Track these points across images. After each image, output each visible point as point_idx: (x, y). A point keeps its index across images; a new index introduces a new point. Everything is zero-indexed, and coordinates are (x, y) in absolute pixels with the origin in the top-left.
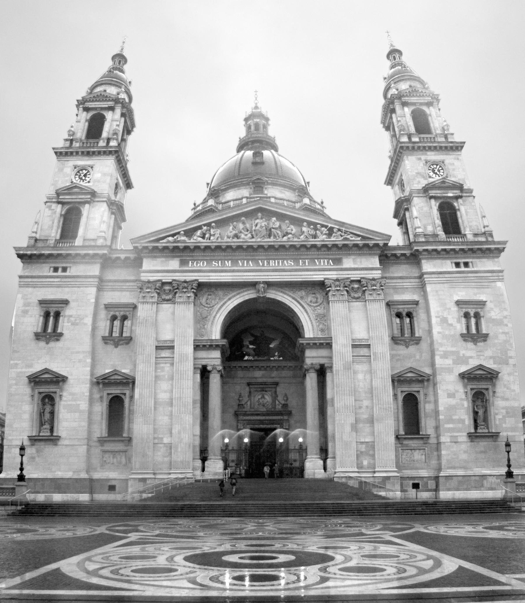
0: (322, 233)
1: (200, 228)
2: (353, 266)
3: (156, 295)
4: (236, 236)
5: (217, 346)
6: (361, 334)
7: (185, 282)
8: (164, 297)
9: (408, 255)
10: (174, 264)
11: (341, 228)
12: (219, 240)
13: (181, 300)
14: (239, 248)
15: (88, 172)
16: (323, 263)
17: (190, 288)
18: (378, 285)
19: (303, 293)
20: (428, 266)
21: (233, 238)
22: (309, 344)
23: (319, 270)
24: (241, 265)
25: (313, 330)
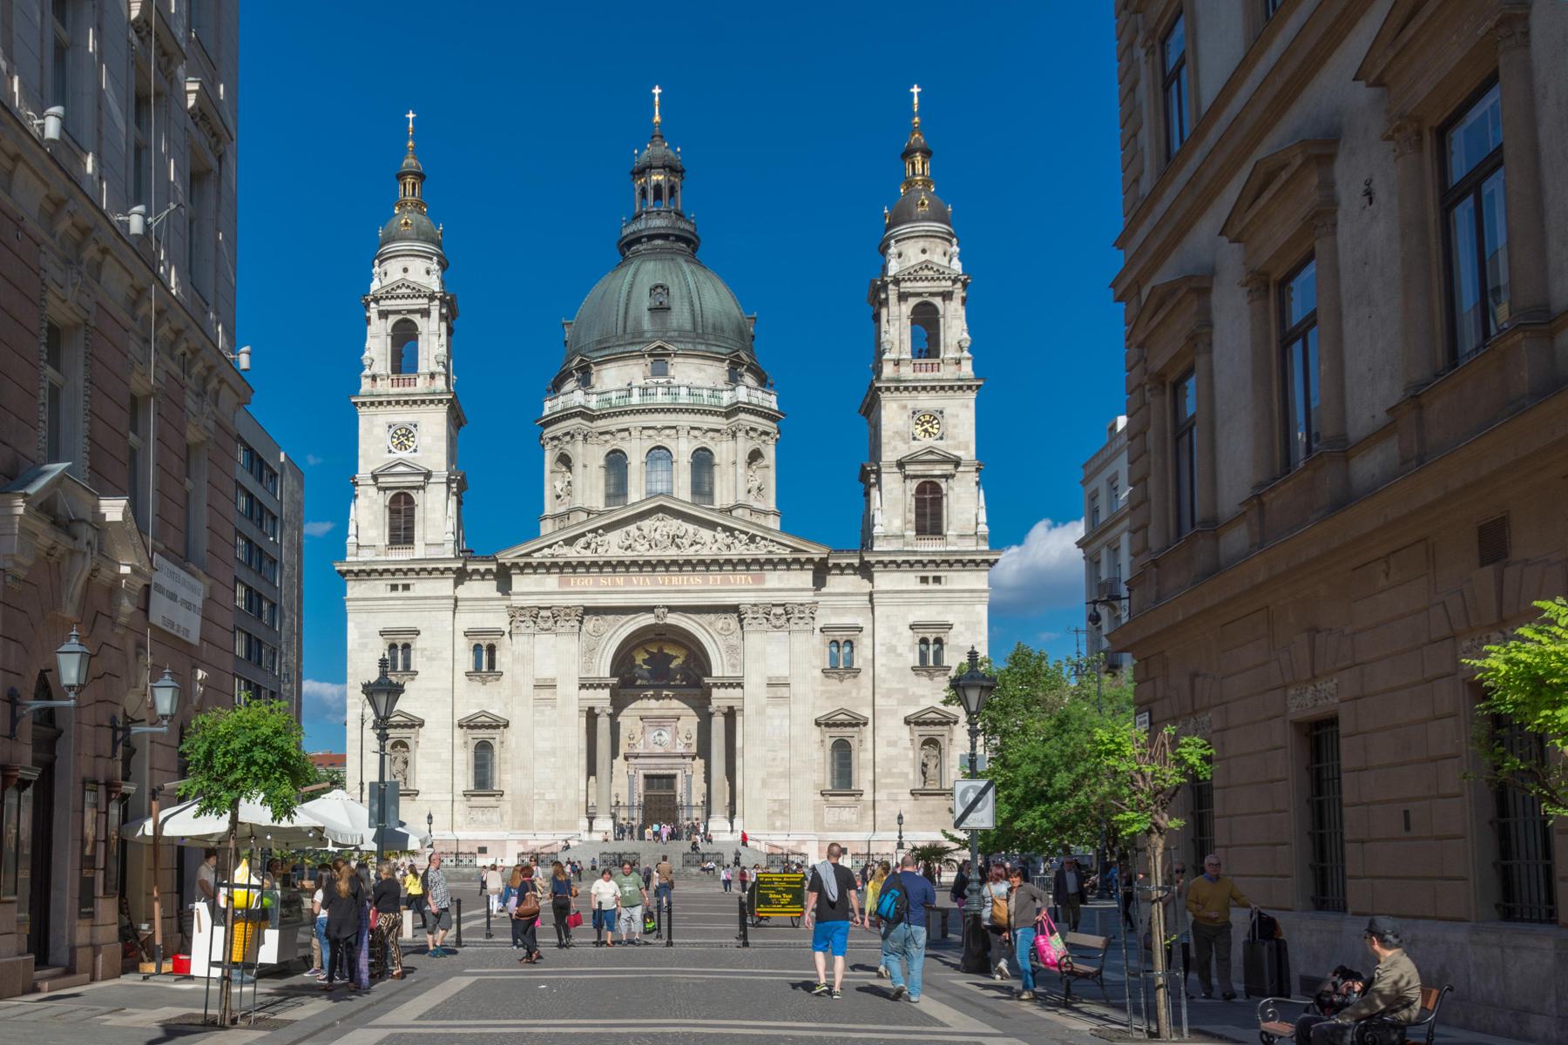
0: (740, 542)
1: (583, 535)
2: (778, 586)
3: (532, 623)
4: (630, 546)
5: (607, 686)
6: (781, 671)
7: (568, 608)
8: (542, 625)
9: (857, 565)
10: (551, 582)
11: (766, 536)
12: (609, 554)
13: (562, 630)
14: (634, 563)
15: (410, 432)
16: (741, 579)
17: (573, 614)
18: (807, 611)
19: (712, 617)
20: (883, 580)
21: (626, 549)
22: (715, 685)
23: (733, 591)
24: (635, 582)
25: (723, 665)
